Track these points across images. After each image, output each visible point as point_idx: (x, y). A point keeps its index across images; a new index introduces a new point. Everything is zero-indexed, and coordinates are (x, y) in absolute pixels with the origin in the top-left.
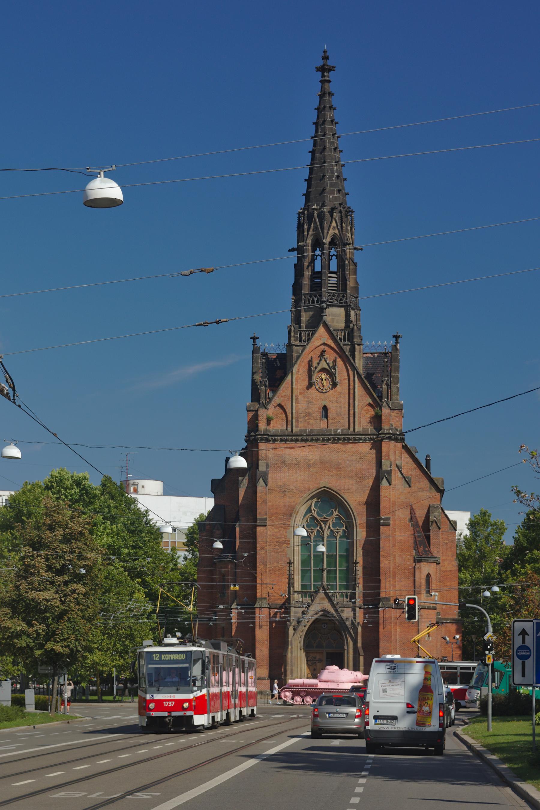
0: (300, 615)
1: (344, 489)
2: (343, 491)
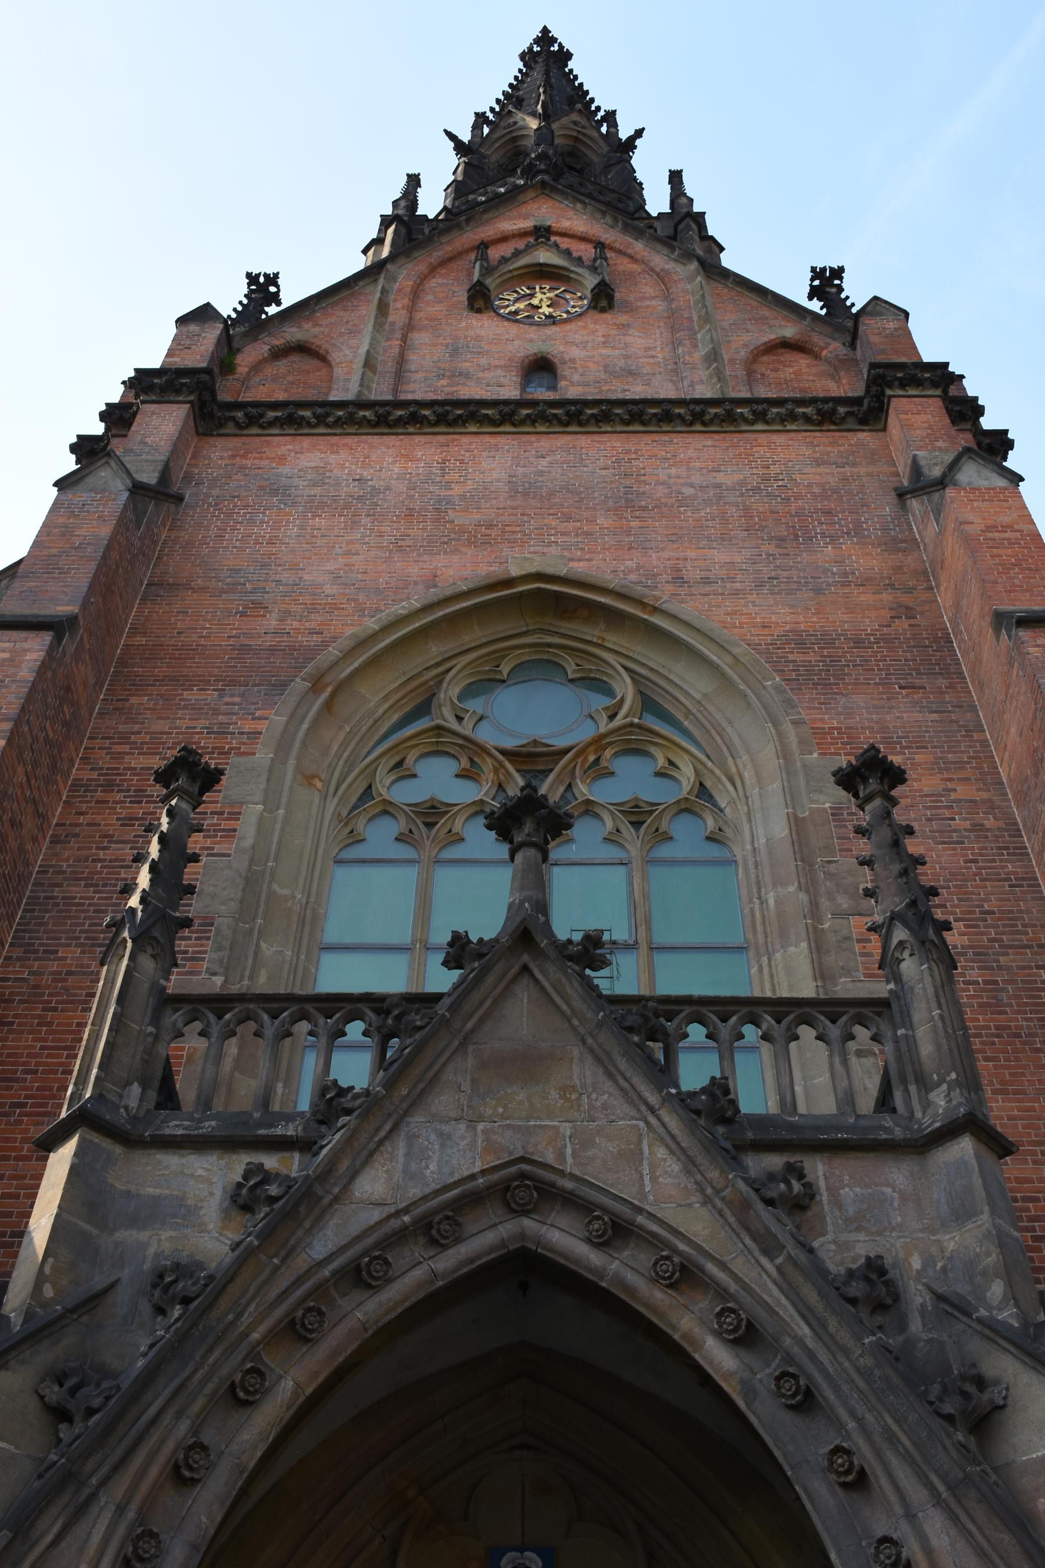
0: (212, 1239)
1: (678, 579)
2: (670, 588)
